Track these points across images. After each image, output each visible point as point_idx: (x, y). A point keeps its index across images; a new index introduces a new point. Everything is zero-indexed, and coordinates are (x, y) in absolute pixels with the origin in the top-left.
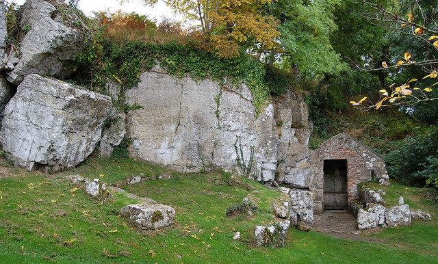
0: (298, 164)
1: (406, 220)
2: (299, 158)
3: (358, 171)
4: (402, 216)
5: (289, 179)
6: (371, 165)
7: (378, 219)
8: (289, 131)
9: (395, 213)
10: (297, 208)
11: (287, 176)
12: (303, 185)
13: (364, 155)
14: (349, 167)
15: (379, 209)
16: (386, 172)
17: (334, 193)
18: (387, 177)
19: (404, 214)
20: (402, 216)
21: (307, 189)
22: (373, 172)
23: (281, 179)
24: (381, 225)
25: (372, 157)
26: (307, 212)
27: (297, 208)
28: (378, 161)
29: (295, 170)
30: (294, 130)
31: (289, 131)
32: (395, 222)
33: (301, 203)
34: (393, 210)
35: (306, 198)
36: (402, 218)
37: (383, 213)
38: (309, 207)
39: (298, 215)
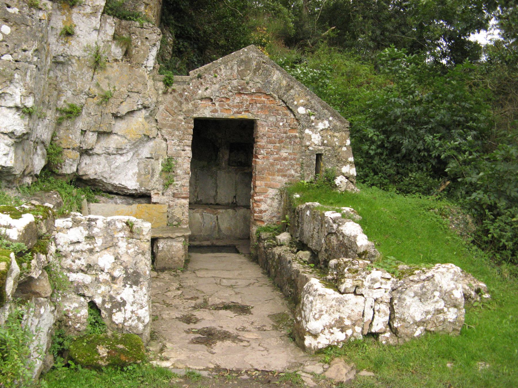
0: (119, 126)
1: (451, 315)
2: (124, 109)
3: (284, 153)
4: (441, 305)
5: (93, 168)
6: (316, 138)
7: (368, 317)
8: (95, 22)
9: (422, 296)
10: (88, 279)
11: (86, 160)
12: (131, 184)
13: (301, 110)
14: (261, 142)
15: (374, 281)
16: (351, 159)
17: (214, 205)
18: (353, 171)
19: (447, 297)
20: (441, 305)
21: (144, 197)
22: (319, 156)
23: (69, 169)
24: (375, 335)
25: (320, 118)
26: (127, 293)
27: (88, 279)
28: (335, 129)
29: (112, 142)
30: (111, 20)
31: (95, 22)
32: (418, 324)
33: (105, 260)
34: (416, 287)
35: (123, 245)
36: (439, 311)
37: (387, 297)
38: (133, 278)
39: (92, 305)
